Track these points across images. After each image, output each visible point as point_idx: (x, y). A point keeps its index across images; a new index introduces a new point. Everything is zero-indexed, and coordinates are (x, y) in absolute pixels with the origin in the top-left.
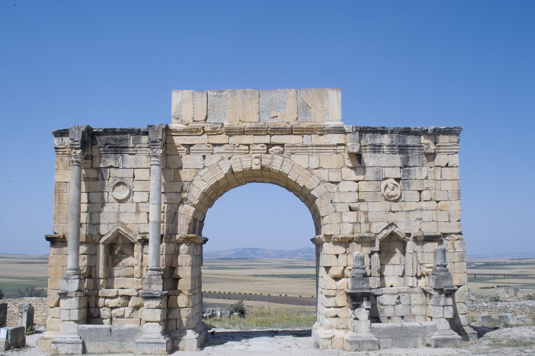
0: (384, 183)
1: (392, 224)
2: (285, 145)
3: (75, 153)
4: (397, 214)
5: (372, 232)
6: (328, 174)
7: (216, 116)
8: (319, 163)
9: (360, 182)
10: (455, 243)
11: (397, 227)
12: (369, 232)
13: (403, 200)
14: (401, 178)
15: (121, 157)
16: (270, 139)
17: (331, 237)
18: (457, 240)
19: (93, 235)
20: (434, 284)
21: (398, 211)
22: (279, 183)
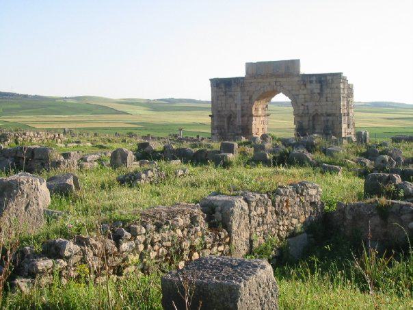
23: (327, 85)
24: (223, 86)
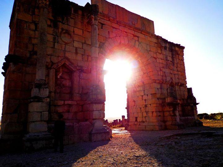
9: (163, 60)
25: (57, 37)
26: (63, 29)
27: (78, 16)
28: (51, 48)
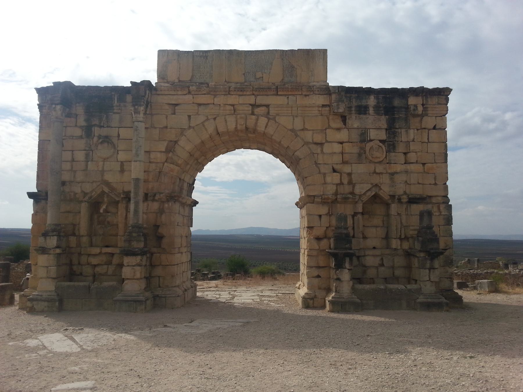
0: (369, 145)
1: (376, 185)
2: (270, 106)
3: (55, 107)
4: (381, 176)
5: (355, 193)
6: (313, 136)
7: (202, 77)
8: (304, 124)
9: (344, 144)
10: (440, 206)
11: (381, 189)
12: (352, 193)
13: (387, 162)
14: (386, 139)
15: (105, 115)
16: (255, 99)
17: (314, 198)
18: (443, 203)
19: (77, 193)
20: (420, 246)
21: (383, 173)
22: (266, 148)
23: (406, 120)
24: (80, 110)
25: (91, 152)
26: (99, 137)
27: (125, 106)
28: (81, 170)
